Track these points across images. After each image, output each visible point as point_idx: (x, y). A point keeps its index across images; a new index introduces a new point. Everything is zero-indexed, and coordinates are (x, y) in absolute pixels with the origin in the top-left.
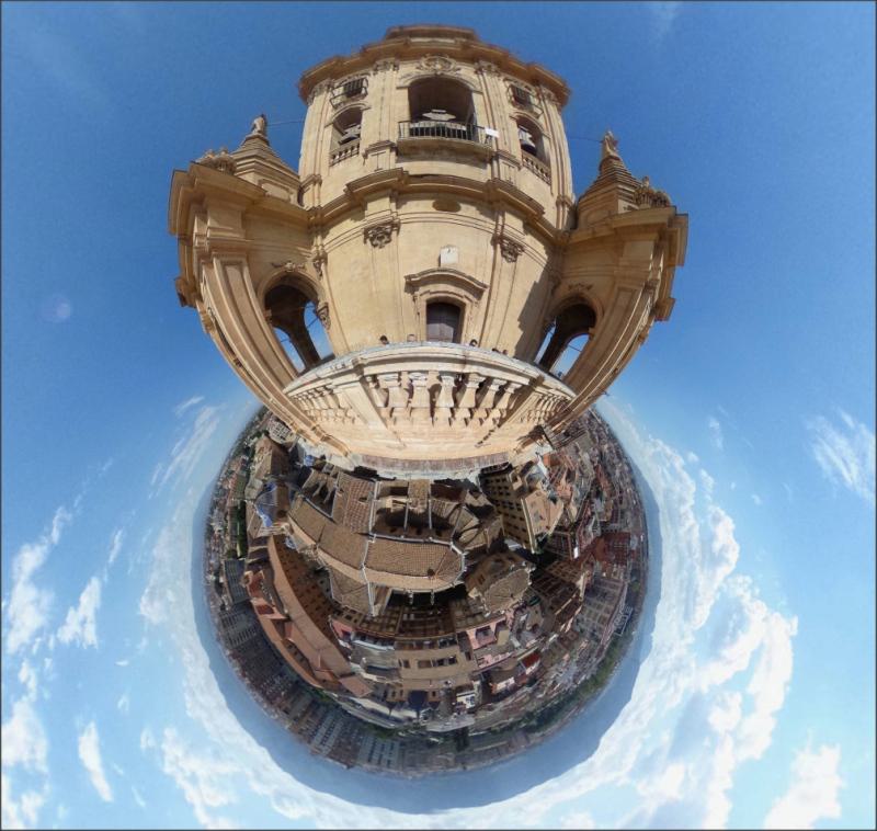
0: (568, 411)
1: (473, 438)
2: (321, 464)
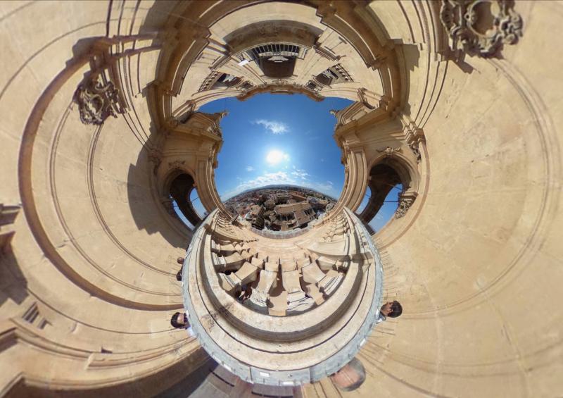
0: (224, 212)
1: (258, 245)
2: (316, 217)
